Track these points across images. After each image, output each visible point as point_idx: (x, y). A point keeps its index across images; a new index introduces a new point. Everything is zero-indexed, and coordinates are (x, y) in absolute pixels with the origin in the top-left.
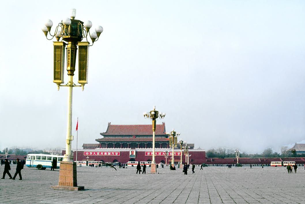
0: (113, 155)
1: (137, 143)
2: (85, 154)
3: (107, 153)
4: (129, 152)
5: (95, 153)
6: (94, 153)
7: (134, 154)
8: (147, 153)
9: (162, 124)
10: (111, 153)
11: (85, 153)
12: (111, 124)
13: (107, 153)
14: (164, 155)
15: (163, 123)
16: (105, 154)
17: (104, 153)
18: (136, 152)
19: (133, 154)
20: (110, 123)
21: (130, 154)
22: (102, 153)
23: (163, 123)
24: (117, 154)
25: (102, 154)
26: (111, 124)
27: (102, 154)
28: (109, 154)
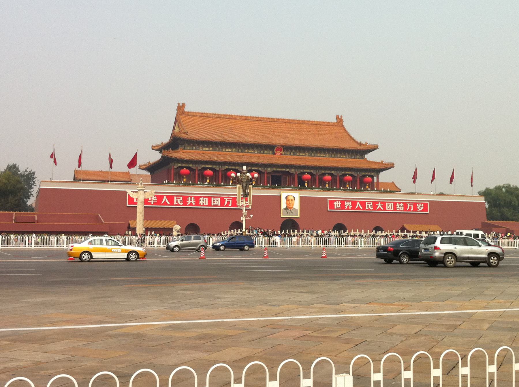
0: (227, 205)
1: (293, 171)
3: (210, 199)
4: (280, 197)
5: (167, 197)
6: (165, 197)
7: (297, 205)
8: (332, 203)
9: (334, 120)
10: (223, 201)
12: (186, 109)
13: (210, 199)
14: (380, 209)
15: (337, 117)
17: (197, 199)
18: (302, 200)
19: (293, 205)
20: (184, 105)
21: (284, 205)
22: (191, 201)
23: (337, 117)
26: (186, 109)
28: (216, 202)
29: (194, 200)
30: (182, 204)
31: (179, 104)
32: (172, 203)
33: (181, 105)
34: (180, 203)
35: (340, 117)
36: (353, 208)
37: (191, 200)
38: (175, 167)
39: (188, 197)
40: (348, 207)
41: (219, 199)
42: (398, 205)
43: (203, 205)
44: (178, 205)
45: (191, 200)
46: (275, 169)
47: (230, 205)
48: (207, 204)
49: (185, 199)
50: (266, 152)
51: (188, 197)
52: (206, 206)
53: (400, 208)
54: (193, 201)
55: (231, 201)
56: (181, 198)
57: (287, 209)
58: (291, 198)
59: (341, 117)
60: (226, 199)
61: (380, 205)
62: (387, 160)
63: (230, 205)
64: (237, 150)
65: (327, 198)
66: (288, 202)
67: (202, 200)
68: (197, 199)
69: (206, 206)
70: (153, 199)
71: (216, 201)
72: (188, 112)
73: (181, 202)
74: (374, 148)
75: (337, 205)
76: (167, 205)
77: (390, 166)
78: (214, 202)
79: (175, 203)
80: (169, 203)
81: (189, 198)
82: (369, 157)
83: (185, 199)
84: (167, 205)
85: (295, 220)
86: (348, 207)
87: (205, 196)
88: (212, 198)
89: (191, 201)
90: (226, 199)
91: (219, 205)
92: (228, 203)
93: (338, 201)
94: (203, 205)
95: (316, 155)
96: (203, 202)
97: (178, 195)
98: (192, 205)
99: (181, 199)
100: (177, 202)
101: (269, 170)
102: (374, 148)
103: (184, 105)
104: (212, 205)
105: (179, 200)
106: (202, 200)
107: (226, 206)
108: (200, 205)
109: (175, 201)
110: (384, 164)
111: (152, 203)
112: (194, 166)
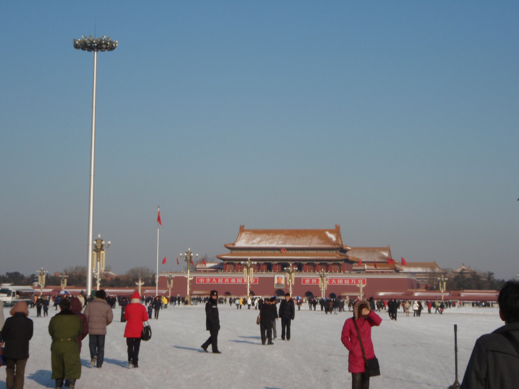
2: (198, 281)
4: (274, 278)
7: (283, 282)
8: (304, 281)
11: (198, 279)
12: (245, 228)
15: (336, 226)
17: (230, 280)
20: (243, 226)
21: (276, 282)
22: (227, 280)
23: (336, 226)
42: (345, 281)
53: (347, 282)
61: (334, 281)
68: (230, 280)
75: (307, 281)
83: (224, 280)
87: (234, 278)
89: (227, 280)
96: (233, 281)
97: (221, 278)
101: (276, 262)
103: (243, 226)
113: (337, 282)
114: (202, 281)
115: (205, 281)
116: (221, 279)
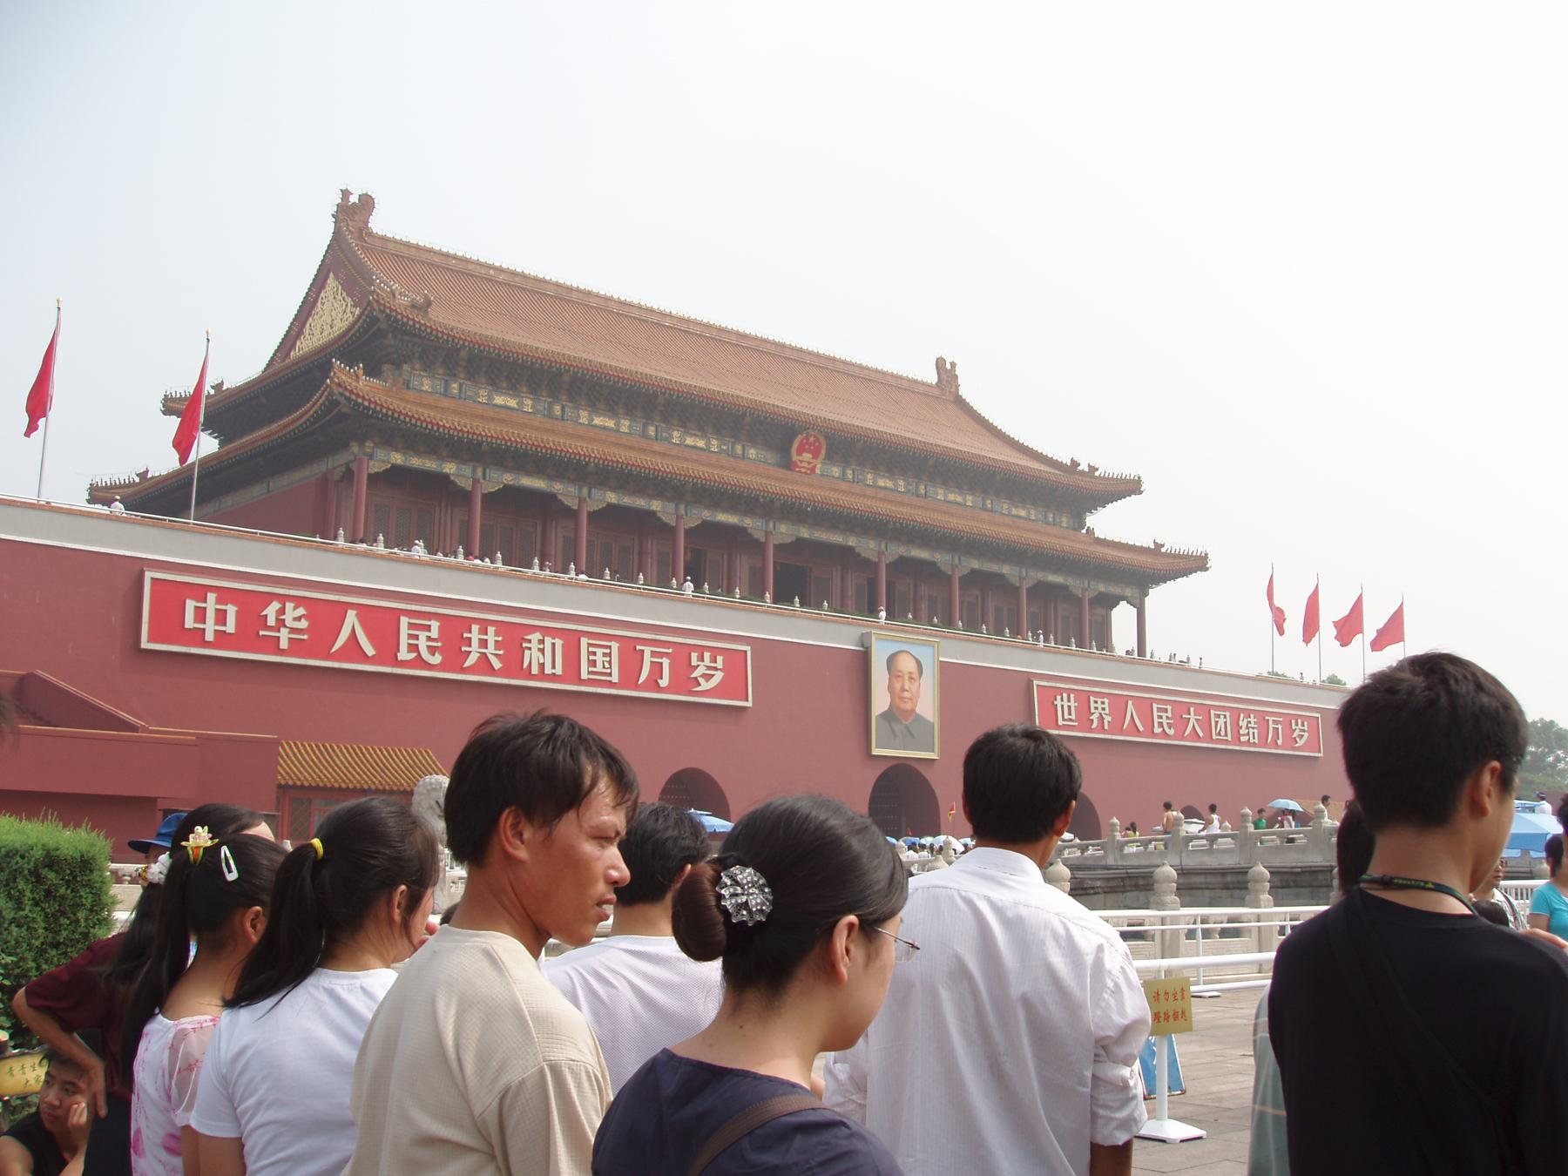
1: (868, 547)
3: (572, 643)
6: (351, 616)
7: (927, 704)
12: (381, 223)
13: (572, 643)
15: (940, 363)
16: (532, 657)
17: (514, 639)
20: (367, 203)
21: (880, 702)
24: (709, 677)
25: (484, 664)
27: (484, 664)
29: (498, 645)
30: (436, 659)
31: (346, 194)
32: (388, 650)
33: (354, 199)
34: (426, 655)
35: (948, 366)
36: (1117, 726)
37: (484, 643)
38: (376, 467)
39: (467, 623)
40: (1101, 718)
41: (615, 646)
43: (542, 676)
44: (420, 662)
45: (484, 643)
46: (805, 533)
47: (664, 682)
48: (559, 671)
49: (454, 635)
50: (752, 453)
51: (467, 623)
52: (553, 678)
54: (491, 645)
55: (666, 662)
56: (435, 625)
57: (888, 716)
58: (906, 665)
59: (953, 365)
60: (647, 650)
62: (1177, 541)
63: (664, 682)
64: (638, 428)
65: (1028, 679)
66: (898, 686)
67: (535, 645)
69: (553, 678)
70: (290, 623)
71: (599, 658)
72: (384, 239)
73: (432, 650)
74: (1131, 487)
76: (365, 658)
77: (1195, 564)
78: (593, 663)
79: (404, 655)
80: (370, 650)
81: (475, 634)
82: (1108, 523)
83: (454, 635)
84: (365, 658)
85: (922, 769)
86: (1101, 718)
88: (584, 641)
89: (482, 645)
90: (647, 650)
91: (615, 678)
92: (657, 669)
93: (1069, 691)
94: (542, 676)
95: (931, 490)
96: (543, 656)
97: (422, 608)
98: (491, 671)
99: (434, 633)
100: (413, 648)
102: (1131, 487)
103: (367, 203)
104: (584, 675)
105: (423, 635)
106: (535, 645)
107: (644, 687)
108: (530, 677)
109: (404, 641)
110: (1168, 555)
111: (284, 644)
112: (467, 470)
113: (1206, 724)
114: (211, 621)
115: (252, 629)
116: (420, 622)
